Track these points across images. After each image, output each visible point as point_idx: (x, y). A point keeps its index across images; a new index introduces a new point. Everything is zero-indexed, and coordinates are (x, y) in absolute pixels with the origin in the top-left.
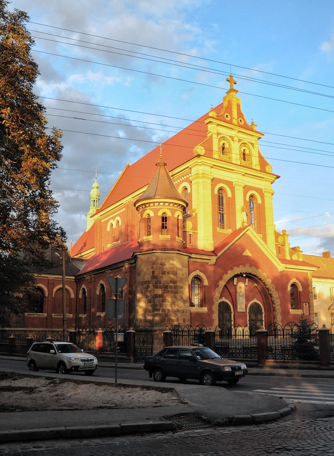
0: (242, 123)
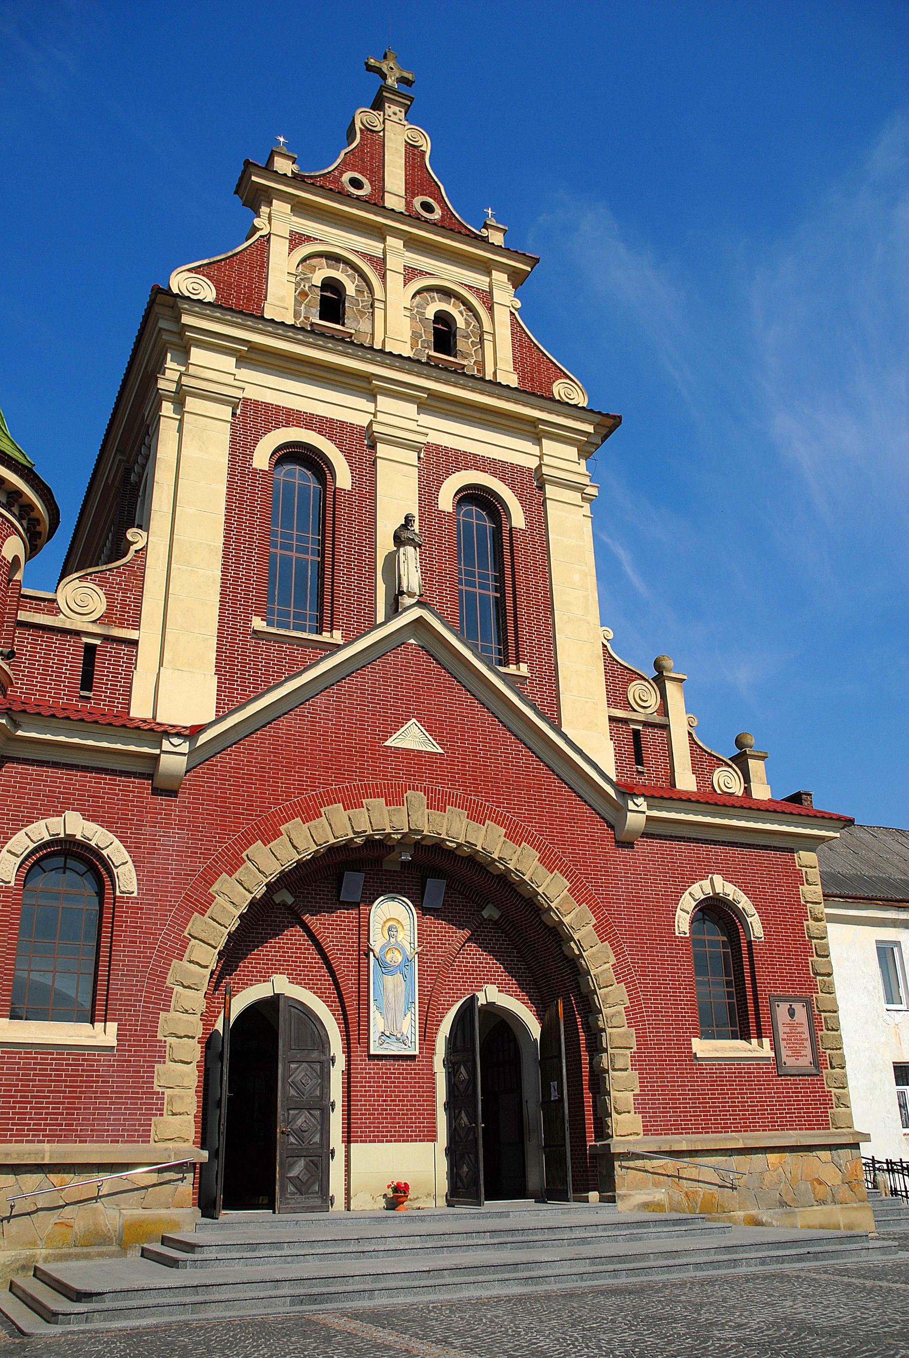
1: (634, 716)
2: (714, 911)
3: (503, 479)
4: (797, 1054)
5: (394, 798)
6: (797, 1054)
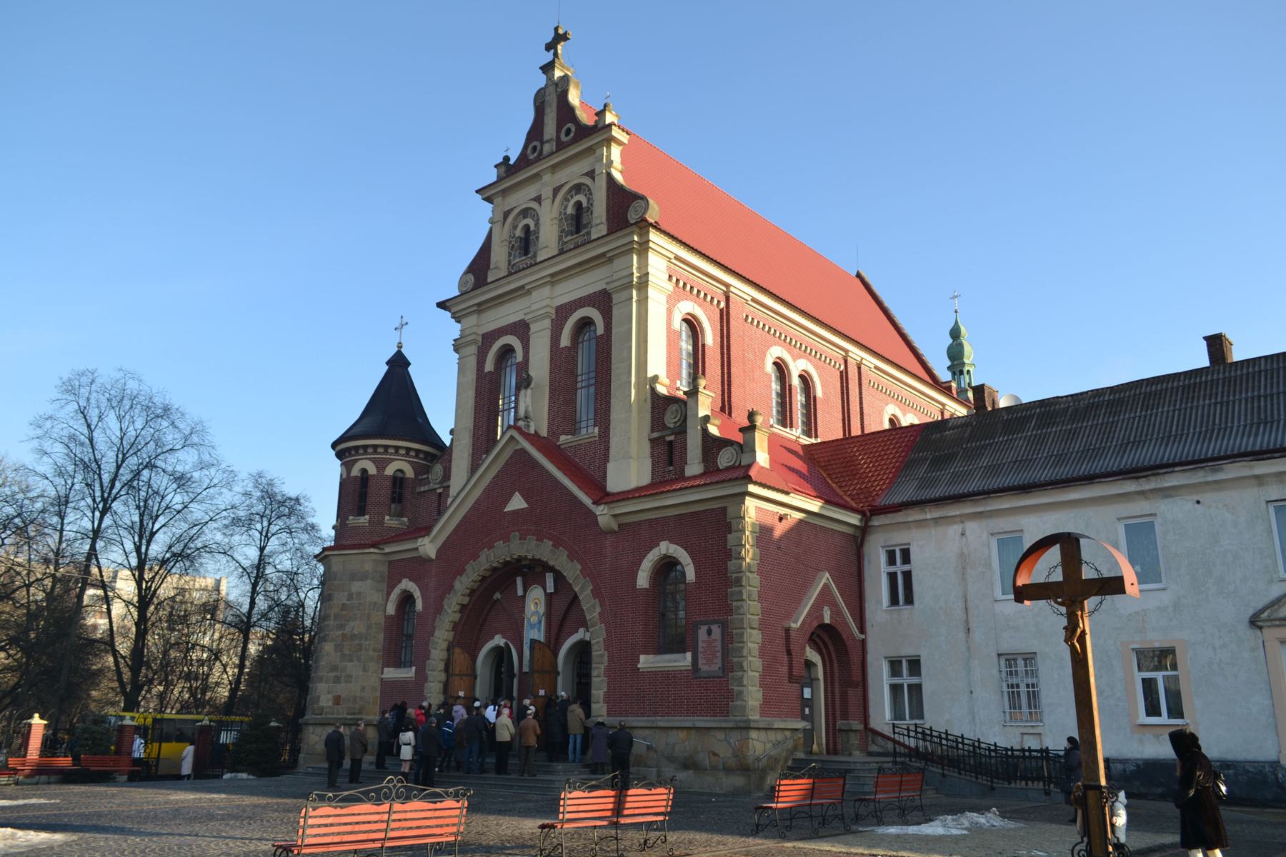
0: (563, 138)
2: (667, 566)
4: (710, 662)
5: (506, 539)
6: (710, 662)
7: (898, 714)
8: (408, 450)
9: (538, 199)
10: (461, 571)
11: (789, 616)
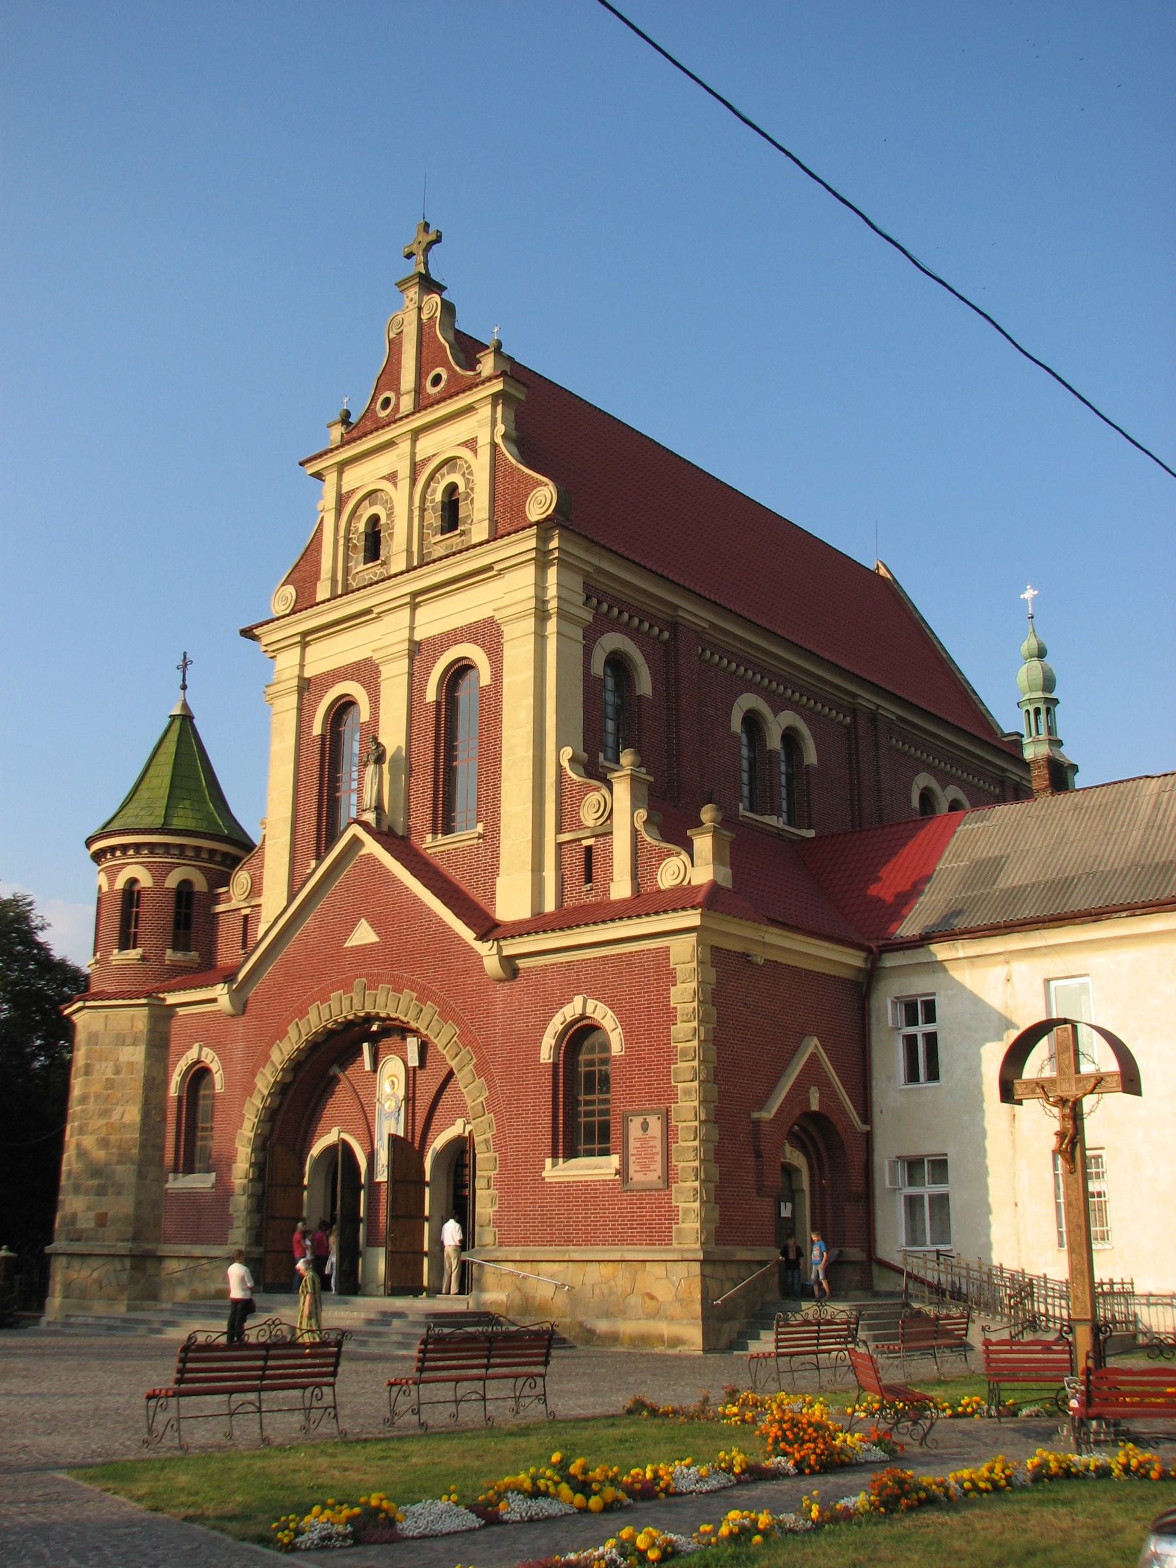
1: (580, 834)
2: (582, 1033)
3: (475, 642)
4: (645, 1169)
5: (347, 987)
6: (645, 1169)
7: (914, 1237)
8: (198, 849)
9: (392, 478)
10: (281, 1034)
11: (761, 1104)
